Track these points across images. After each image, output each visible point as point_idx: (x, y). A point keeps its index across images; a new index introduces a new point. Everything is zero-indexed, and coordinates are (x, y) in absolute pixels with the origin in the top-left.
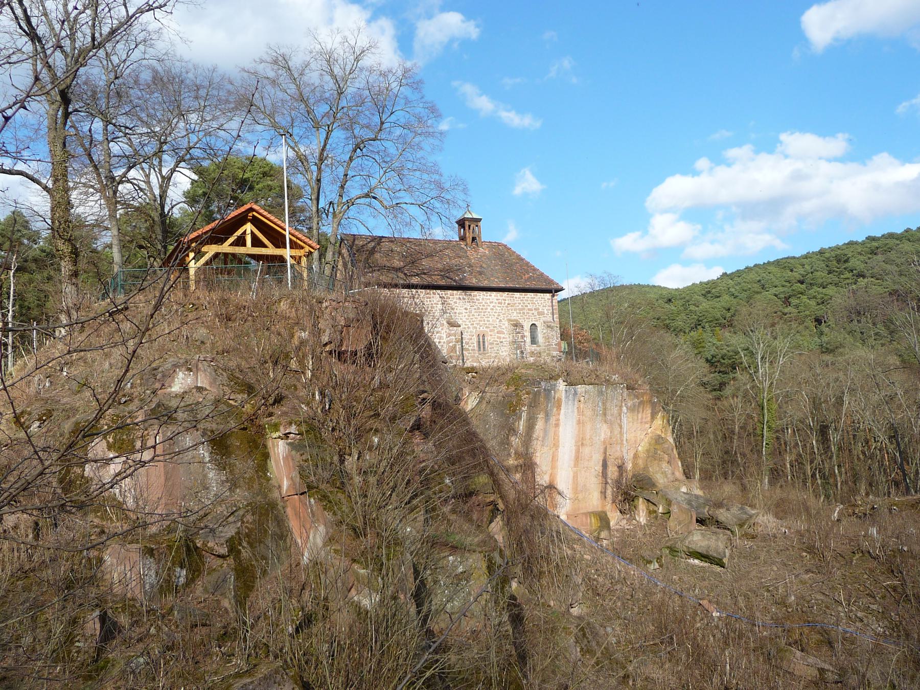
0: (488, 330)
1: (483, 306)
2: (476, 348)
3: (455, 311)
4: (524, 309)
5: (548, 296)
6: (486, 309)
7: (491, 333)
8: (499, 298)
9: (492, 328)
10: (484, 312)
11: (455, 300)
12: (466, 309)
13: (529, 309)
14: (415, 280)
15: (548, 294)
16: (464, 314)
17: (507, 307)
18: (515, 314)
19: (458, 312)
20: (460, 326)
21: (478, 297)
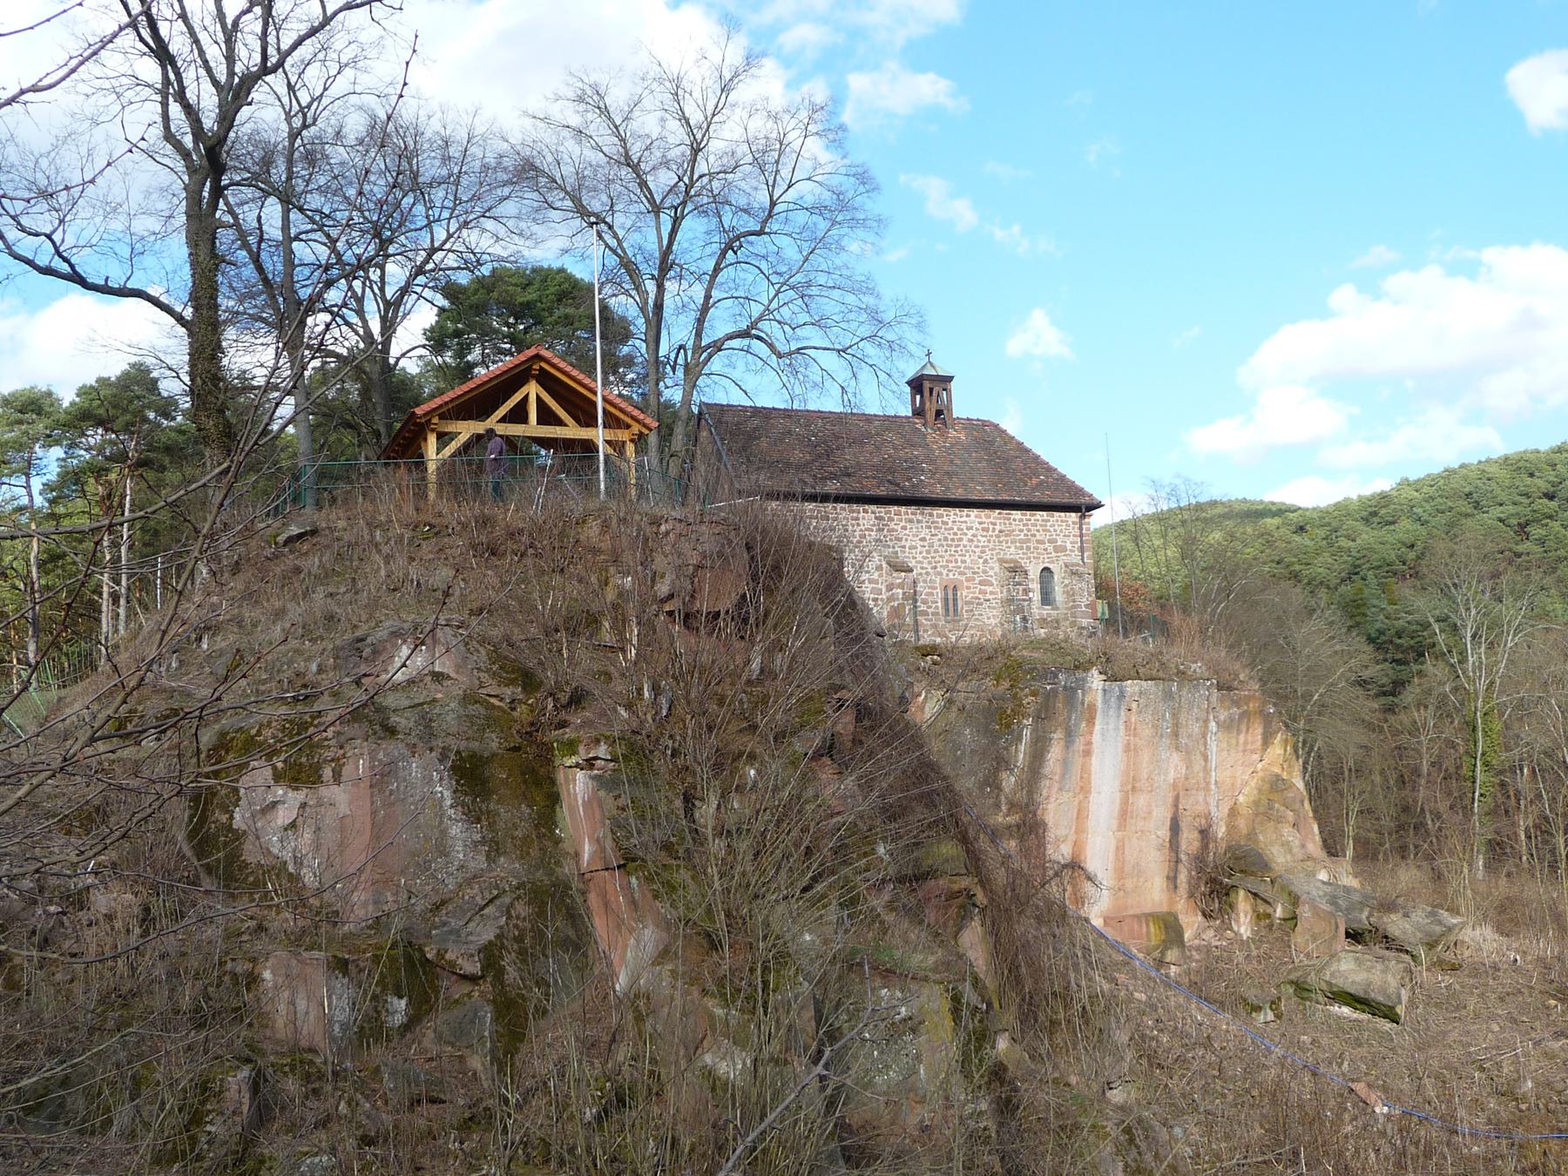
0: (963, 578)
1: (955, 534)
3: (903, 543)
4: (1029, 541)
5: (1073, 516)
6: (961, 540)
7: (970, 584)
10: (957, 546)
11: (903, 524)
13: (1038, 542)
14: (832, 487)
15: (1073, 514)
16: (919, 549)
17: (998, 536)
18: (1013, 549)
19: (908, 544)
20: (911, 571)
21: (945, 519)
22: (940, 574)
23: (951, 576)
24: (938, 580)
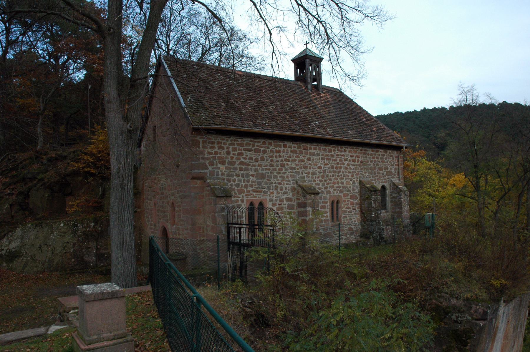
1: (338, 164)
2: (329, 218)
4: (375, 168)
5: (395, 153)
6: (341, 168)
7: (345, 198)
8: (353, 154)
9: (346, 192)
10: (339, 172)
11: (308, 156)
12: (320, 168)
13: (381, 169)
16: (318, 174)
17: (360, 165)
18: (367, 174)
19: (311, 171)
21: (333, 153)
22: (329, 192)
23: (336, 194)
24: (328, 196)
